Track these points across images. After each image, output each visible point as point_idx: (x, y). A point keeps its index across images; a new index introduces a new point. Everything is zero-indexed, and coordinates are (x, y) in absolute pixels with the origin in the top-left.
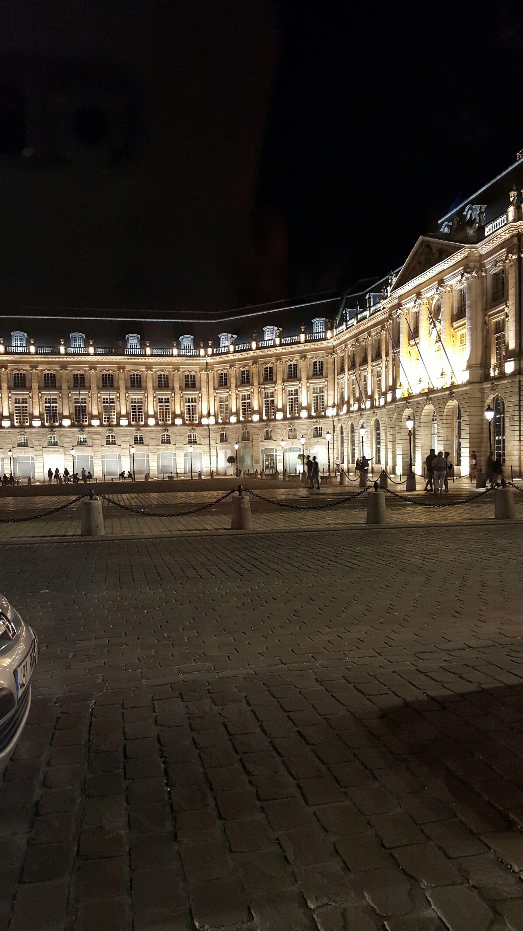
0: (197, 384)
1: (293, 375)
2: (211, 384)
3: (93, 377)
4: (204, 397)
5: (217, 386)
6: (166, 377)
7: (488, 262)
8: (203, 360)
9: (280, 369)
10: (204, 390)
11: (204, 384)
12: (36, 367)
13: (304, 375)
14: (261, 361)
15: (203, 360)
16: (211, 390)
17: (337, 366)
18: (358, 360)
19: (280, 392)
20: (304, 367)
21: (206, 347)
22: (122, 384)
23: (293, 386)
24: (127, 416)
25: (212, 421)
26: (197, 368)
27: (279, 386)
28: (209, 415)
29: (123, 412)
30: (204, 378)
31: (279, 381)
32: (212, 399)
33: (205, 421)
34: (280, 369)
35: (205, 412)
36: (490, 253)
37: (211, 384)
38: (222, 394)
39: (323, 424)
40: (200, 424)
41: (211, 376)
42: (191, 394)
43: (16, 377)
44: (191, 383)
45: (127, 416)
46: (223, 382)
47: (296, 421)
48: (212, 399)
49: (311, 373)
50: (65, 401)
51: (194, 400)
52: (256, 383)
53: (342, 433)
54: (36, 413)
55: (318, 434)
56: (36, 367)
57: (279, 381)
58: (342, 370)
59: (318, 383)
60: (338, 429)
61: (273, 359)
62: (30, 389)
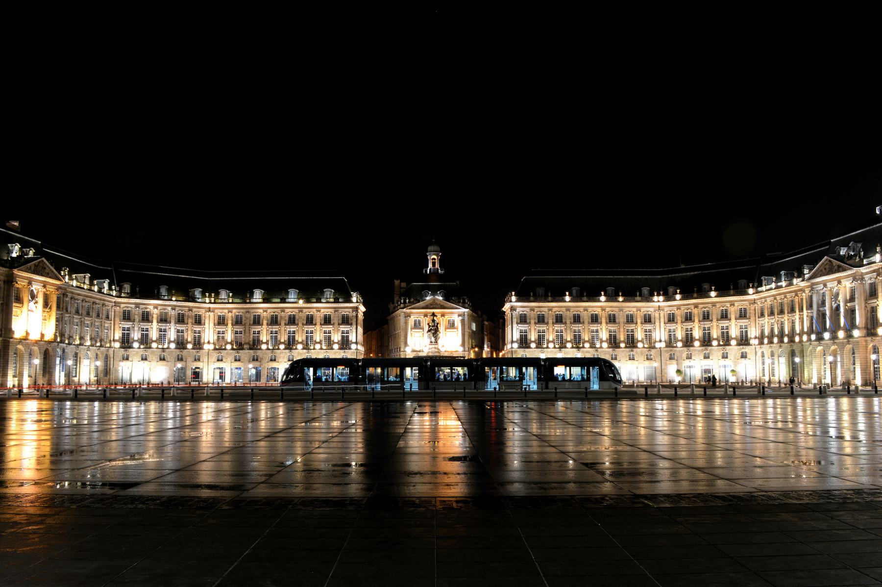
0: (653, 320)
1: (725, 316)
2: (662, 320)
3: (586, 316)
5: (666, 320)
6: (632, 316)
7: (867, 277)
8: (657, 304)
9: (715, 313)
10: (657, 324)
11: (657, 321)
12: (551, 310)
13: (733, 317)
14: (701, 306)
15: (657, 304)
16: (662, 324)
17: (758, 312)
18: (776, 311)
19: (715, 327)
20: (733, 312)
21: (658, 295)
22: (604, 320)
23: (725, 323)
25: (663, 345)
26: (652, 310)
27: (715, 323)
28: (660, 341)
30: (657, 315)
31: (715, 320)
32: (663, 330)
33: (658, 345)
34: (715, 313)
35: (658, 339)
36: (867, 273)
37: (662, 320)
38: (672, 326)
39: (747, 349)
40: (654, 347)
41: (662, 315)
42: (648, 327)
43: (539, 316)
44: (648, 320)
46: (671, 319)
47: (728, 347)
48: (663, 330)
49: (738, 315)
50: (569, 331)
51: (650, 331)
52: (697, 321)
53: (763, 356)
54: (551, 339)
55: (744, 356)
56: (551, 310)
57: (715, 320)
58: (762, 315)
59: (743, 322)
60: (759, 354)
61: (710, 306)
62: (547, 324)
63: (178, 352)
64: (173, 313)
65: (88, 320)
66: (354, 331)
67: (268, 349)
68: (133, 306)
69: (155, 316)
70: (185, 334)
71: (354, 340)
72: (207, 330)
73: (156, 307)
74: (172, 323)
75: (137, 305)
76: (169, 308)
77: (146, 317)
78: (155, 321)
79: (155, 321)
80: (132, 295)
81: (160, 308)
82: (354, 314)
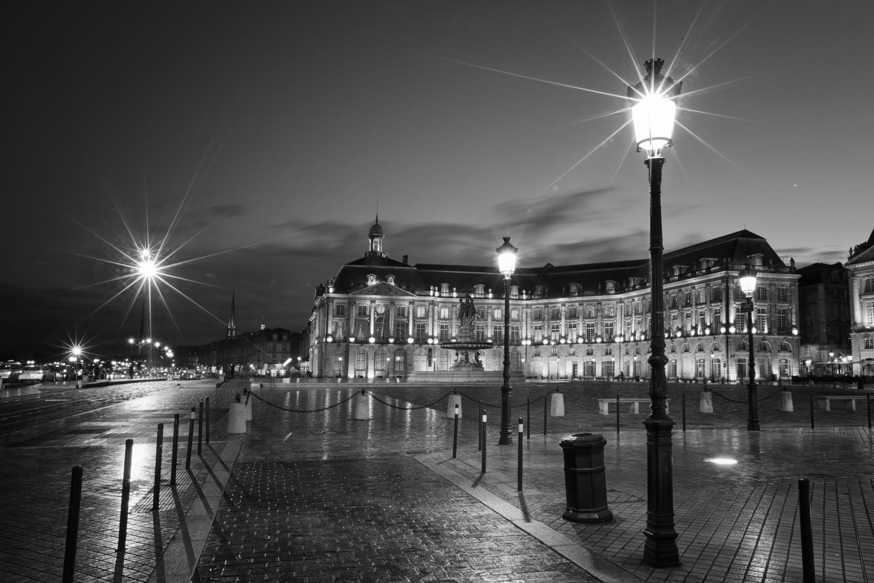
4: (524, 328)
24: (583, 337)
29: (581, 334)
45: (583, 337)
63: (586, 346)
64: (581, 308)
65: (687, 311)
66: (724, 309)
67: (566, 343)
68: (543, 306)
69: (563, 313)
70: (595, 328)
71: (724, 321)
72: (524, 328)
73: (563, 305)
74: (581, 319)
75: (546, 305)
76: (577, 304)
77: (556, 316)
78: (563, 318)
79: (563, 318)
80: (543, 296)
81: (567, 305)
82: (724, 286)
